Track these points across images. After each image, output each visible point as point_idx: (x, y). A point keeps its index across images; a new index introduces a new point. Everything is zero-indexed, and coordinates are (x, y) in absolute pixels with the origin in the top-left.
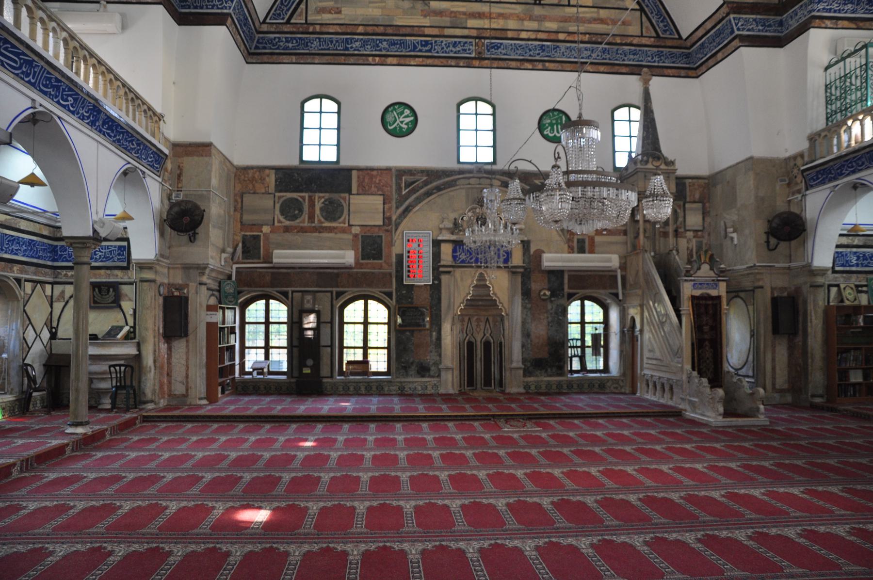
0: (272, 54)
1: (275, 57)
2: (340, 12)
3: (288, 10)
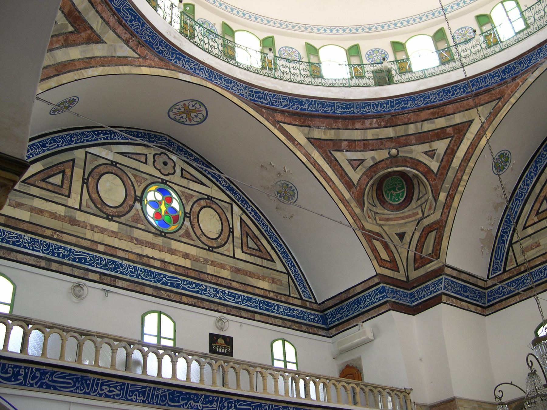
0: (501, 301)
1: (503, 303)
2: (539, 245)
3: (501, 262)
